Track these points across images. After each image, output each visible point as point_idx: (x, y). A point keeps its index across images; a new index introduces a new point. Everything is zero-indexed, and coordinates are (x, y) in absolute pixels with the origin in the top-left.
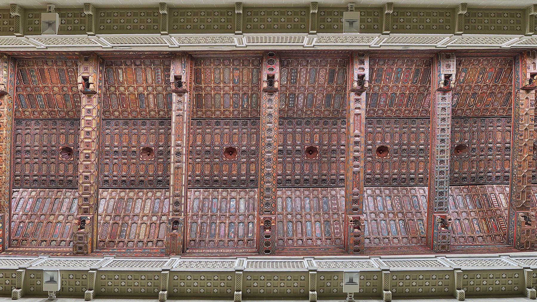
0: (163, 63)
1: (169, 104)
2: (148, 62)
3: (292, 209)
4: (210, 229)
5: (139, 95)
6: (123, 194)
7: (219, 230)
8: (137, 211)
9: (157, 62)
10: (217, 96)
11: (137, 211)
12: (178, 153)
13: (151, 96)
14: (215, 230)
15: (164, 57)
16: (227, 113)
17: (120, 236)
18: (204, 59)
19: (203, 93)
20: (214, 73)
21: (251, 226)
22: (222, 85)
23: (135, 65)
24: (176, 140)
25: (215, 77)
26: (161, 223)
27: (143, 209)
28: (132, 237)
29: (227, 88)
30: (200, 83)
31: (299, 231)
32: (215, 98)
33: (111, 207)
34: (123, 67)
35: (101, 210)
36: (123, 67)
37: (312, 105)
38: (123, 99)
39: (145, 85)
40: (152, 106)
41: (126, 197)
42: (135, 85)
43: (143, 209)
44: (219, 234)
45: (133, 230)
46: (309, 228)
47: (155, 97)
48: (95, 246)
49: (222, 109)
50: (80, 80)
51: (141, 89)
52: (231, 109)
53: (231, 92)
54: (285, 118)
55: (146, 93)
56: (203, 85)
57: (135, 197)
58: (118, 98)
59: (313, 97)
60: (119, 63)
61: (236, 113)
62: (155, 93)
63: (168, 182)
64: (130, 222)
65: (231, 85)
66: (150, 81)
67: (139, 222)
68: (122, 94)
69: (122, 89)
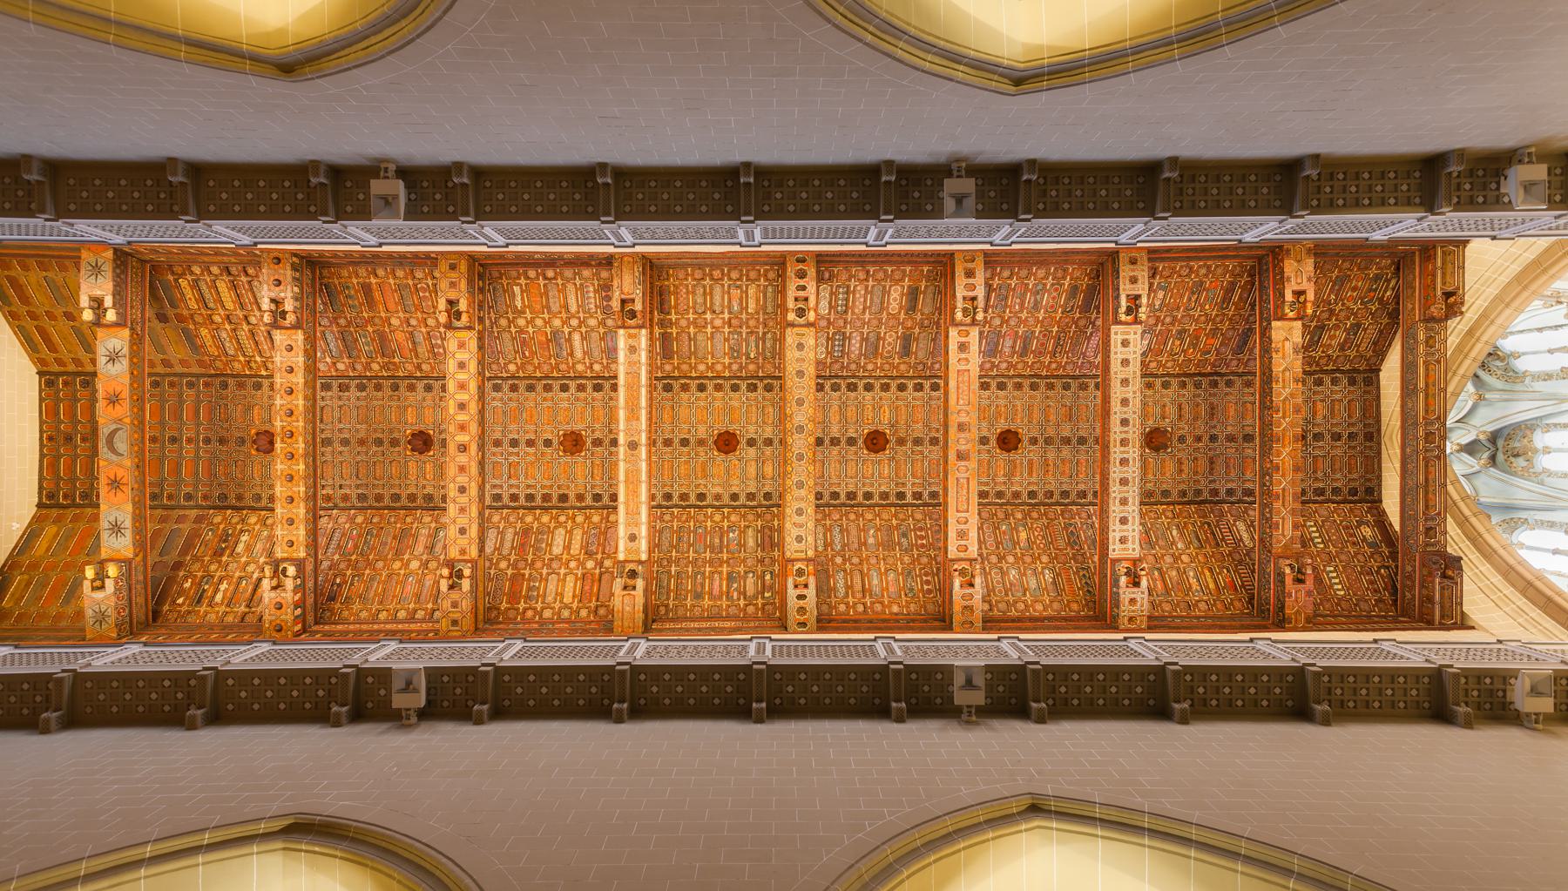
0: (597, 275)
1: (611, 353)
2: (568, 273)
3: (844, 546)
4: (694, 585)
5: (555, 333)
6: (529, 519)
7: (711, 584)
8: (557, 550)
9: (586, 273)
10: (700, 337)
11: (557, 550)
12: (633, 446)
13: (576, 337)
14: (703, 585)
15: (600, 264)
16: (719, 367)
17: (528, 598)
18: (675, 267)
19: (674, 331)
20: (694, 293)
21: (768, 577)
22: (708, 316)
23: (545, 278)
24: (628, 420)
25: (695, 302)
26: (601, 574)
27: (567, 547)
28: (550, 599)
29: (718, 323)
30: (669, 313)
31: (858, 587)
32: (695, 339)
33: (508, 545)
34: (523, 281)
35: (488, 550)
36: (523, 281)
37: (876, 353)
38: (524, 342)
39: (564, 315)
40: (579, 354)
41: (535, 525)
42: (546, 316)
43: (567, 547)
44: (710, 593)
45: (552, 587)
46: (875, 582)
47: (583, 338)
48: (481, 617)
49: (710, 361)
50: (442, 305)
51: (557, 323)
52: (727, 361)
53: (726, 330)
54: (827, 379)
55: (566, 330)
56: (674, 317)
57: (553, 525)
58: (514, 339)
59: (879, 338)
60: (514, 274)
61: (735, 367)
62: (583, 330)
63: (614, 497)
64: (545, 571)
65: (726, 316)
66: (573, 309)
67: (563, 571)
68: (521, 331)
69: (521, 322)
